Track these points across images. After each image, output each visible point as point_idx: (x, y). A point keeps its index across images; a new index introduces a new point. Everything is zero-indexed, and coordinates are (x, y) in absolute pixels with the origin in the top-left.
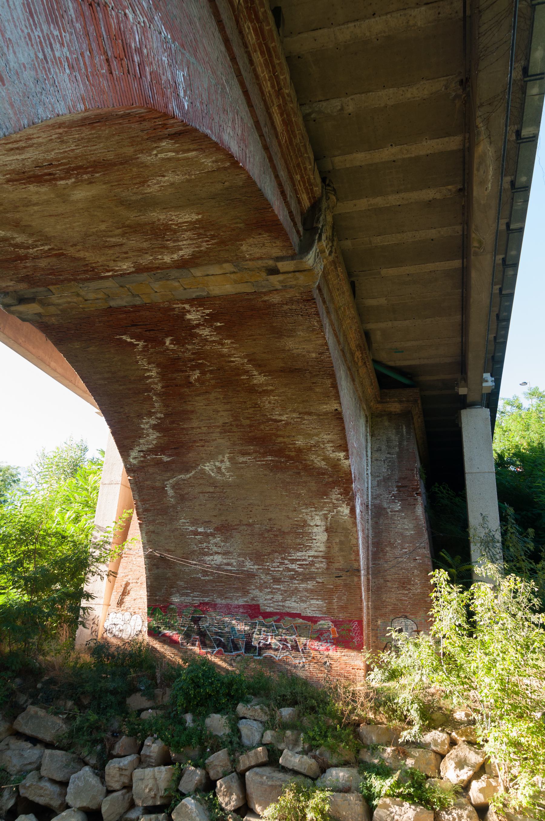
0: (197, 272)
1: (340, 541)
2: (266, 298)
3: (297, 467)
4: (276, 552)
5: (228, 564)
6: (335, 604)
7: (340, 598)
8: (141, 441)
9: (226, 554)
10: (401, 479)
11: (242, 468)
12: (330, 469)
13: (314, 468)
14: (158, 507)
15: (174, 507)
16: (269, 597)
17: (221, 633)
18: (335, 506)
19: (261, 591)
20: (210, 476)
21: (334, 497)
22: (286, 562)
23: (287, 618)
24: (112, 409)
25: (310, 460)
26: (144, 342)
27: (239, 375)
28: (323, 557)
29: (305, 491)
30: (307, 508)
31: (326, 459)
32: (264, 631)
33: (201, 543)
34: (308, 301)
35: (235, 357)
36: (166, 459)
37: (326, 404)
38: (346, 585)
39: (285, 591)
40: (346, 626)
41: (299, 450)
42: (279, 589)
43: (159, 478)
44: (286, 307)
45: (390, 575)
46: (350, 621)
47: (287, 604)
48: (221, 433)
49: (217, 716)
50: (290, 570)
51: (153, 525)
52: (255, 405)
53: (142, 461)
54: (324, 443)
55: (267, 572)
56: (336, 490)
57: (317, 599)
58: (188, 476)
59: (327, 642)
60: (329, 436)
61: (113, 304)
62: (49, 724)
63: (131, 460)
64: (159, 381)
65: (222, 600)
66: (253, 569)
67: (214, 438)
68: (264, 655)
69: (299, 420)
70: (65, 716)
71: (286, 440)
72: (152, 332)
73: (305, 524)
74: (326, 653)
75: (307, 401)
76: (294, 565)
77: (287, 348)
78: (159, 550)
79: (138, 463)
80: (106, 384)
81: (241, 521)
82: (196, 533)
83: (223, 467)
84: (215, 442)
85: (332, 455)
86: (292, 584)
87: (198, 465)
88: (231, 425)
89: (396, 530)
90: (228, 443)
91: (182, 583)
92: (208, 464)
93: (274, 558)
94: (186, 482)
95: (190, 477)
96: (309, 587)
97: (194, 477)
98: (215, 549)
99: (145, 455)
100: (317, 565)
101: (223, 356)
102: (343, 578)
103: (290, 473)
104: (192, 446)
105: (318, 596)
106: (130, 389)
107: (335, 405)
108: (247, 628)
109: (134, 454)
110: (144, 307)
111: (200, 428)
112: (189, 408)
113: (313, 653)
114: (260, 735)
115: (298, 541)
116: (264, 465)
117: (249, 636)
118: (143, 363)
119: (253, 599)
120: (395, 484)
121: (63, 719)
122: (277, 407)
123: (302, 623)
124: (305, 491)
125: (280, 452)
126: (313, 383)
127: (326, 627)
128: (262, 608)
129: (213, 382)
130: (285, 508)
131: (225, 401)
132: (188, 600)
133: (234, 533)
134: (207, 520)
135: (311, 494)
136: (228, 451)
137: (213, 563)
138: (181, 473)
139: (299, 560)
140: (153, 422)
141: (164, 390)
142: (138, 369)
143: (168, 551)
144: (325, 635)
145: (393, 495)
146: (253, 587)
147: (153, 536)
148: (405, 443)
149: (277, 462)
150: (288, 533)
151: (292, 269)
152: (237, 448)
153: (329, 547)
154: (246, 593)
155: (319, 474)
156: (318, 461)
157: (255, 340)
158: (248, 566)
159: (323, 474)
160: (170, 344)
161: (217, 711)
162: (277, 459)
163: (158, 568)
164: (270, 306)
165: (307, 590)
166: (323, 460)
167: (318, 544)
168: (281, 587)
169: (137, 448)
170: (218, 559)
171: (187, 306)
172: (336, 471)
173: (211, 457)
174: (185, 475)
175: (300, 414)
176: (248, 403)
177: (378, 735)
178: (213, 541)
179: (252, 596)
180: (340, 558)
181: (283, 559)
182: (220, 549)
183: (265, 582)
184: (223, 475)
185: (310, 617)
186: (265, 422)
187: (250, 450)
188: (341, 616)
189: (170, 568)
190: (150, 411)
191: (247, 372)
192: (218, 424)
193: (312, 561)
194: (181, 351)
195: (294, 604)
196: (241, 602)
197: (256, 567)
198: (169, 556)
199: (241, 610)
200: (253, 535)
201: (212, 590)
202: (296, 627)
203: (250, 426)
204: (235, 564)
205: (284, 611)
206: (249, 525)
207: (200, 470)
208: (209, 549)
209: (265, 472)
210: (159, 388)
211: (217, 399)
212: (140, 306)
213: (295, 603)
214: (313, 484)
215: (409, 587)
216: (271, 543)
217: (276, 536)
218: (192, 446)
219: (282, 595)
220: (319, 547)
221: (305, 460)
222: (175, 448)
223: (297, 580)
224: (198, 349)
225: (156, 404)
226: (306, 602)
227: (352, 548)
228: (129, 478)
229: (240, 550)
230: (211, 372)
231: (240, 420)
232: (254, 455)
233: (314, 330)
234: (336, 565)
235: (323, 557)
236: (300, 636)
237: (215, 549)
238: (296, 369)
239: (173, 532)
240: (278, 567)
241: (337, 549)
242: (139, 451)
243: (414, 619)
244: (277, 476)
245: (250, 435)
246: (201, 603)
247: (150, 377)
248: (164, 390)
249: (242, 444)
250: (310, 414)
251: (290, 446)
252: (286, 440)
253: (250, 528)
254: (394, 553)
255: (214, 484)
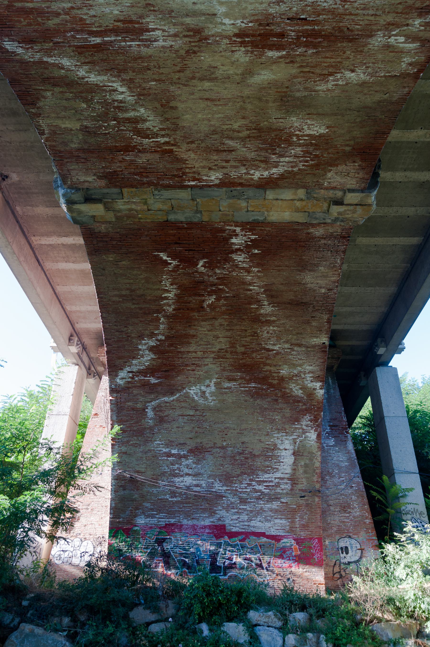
0: (270, 195)
1: (305, 464)
2: (312, 230)
3: (276, 395)
4: (245, 474)
5: (197, 486)
6: (298, 523)
7: (302, 518)
8: (134, 362)
9: (196, 475)
10: (332, 420)
11: (226, 393)
12: (305, 397)
13: (292, 396)
14: (135, 428)
15: (151, 428)
16: (235, 517)
17: (186, 554)
18: (304, 432)
19: (227, 511)
20: (193, 400)
21: (304, 423)
22: (254, 483)
23: (252, 538)
24: (115, 327)
25: (289, 389)
26: (178, 262)
27: (250, 304)
28: (289, 479)
29: (279, 417)
30: (278, 433)
31: (304, 388)
32: (229, 551)
33: (172, 465)
34: (344, 237)
35: (254, 286)
36: (153, 381)
37: (317, 337)
38: (307, 505)
39: (251, 511)
40: (307, 544)
41: (282, 379)
42: (245, 510)
43: (142, 399)
44: (323, 241)
45: (332, 500)
46: (311, 539)
47: (253, 523)
48: (214, 358)
49: (232, 625)
50: (256, 491)
51: (126, 446)
52: (255, 334)
53: (129, 382)
54: (305, 373)
55: (235, 493)
56: (308, 417)
57: (281, 519)
58: (172, 399)
59: (290, 560)
60: (311, 368)
61: (172, 217)
62: (50, 642)
63: (118, 381)
64: (174, 303)
65: (188, 520)
66: (221, 490)
67: (206, 363)
68: (229, 574)
69: (289, 350)
70: (65, 633)
71: (272, 368)
72: (191, 253)
73: (275, 447)
74: (289, 570)
75: (301, 334)
76: (260, 487)
77: (304, 282)
78: (129, 471)
79: (124, 384)
80: (119, 301)
81: (215, 444)
82: (169, 455)
83: (208, 391)
84: (206, 367)
85: (310, 385)
86: (258, 504)
87: (184, 388)
88: (226, 352)
89: (333, 462)
90: (218, 369)
91: (148, 505)
92: (194, 388)
93: (243, 479)
94: (168, 404)
95: (174, 400)
96: (274, 507)
97: (177, 400)
98: (186, 470)
99: (133, 375)
100: (283, 487)
101: (244, 283)
102: (306, 498)
103: (269, 399)
104: (183, 369)
105: (282, 515)
106: (141, 309)
107: (324, 339)
108: (213, 548)
109: (122, 374)
110: (200, 225)
111: (196, 352)
112: (192, 332)
113: (277, 570)
114: (282, 640)
115: (267, 463)
116: (247, 391)
117: (214, 556)
118: (166, 283)
119: (219, 520)
120: (327, 424)
121: (64, 636)
122: (273, 337)
123: (266, 542)
124: (279, 417)
125: (264, 380)
126: (312, 317)
127: (288, 545)
128: (228, 528)
129: (224, 308)
130: (259, 432)
131: (228, 328)
132: (154, 521)
133: (207, 455)
134: (182, 442)
135: (284, 420)
136: (217, 376)
137: (182, 484)
138: (165, 395)
139: (266, 481)
140: (152, 343)
141: (174, 312)
142: (159, 289)
143: (138, 472)
144: (288, 552)
145: (327, 432)
146: (220, 508)
147: (124, 456)
148: (332, 391)
149: (259, 388)
150: (258, 456)
151: (356, 202)
152: (226, 374)
153: (294, 470)
154: (212, 513)
155: (295, 401)
156: (296, 390)
157: (279, 271)
158: (217, 488)
159: (299, 402)
160: (202, 266)
161: (230, 620)
162: (259, 386)
163: (124, 490)
164: (310, 238)
165: (271, 510)
166: (301, 389)
167: (285, 467)
168: (247, 507)
169: (128, 369)
170: (188, 480)
171: (238, 229)
172: (310, 400)
173: (199, 380)
174: (169, 397)
175: (291, 345)
176: (248, 331)
177: (393, 631)
178: (185, 462)
179: (219, 516)
180: (304, 480)
181: (251, 480)
182: (191, 470)
183: (232, 503)
184: (206, 399)
185: (273, 536)
186: (258, 351)
187: (237, 376)
188: (303, 534)
189: (138, 490)
190: (153, 333)
191: (258, 302)
192: (214, 350)
193: (278, 483)
194: (208, 275)
195: (259, 524)
196: (207, 522)
197: (225, 488)
198: (140, 478)
199: (207, 531)
200: (225, 457)
201: (179, 511)
202: (260, 546)
203: (244, 353)
204: (204, 485)
205: (249, 531)
206: (223, 448)
207: (185, 393)
208: (180, 470)
209: (247, 398)
210: (171, 310)
211: (221, 325)
212: (195, 224)
213: (260, 523)
214: (288, 411)
215: (349, 510)
216: (242, 465)
217: (246, 458)
218: (183, 369)
219: (247, 515)
220: (285, 469)
221: (285, 388)
222: (166, 371)
223: (263, 501)
224: (226, 274)
225: (161, 326)
226: (270, 521)
227: (315, 470)
228: (111, 398)
229: (211, 471)
230: (226, 298)
231: (236, 347)
232: (240, 381)
233: (334, 266)
234: (300, 486)
235: (289, 479)
236: (264, 554)
237: (186, 470)
238: (302, 303)
239: (146, 453)
240: (246, 488)
241: (301, 471)
242: (129, 372)
243: (357, 539)
244: (256, 402)
245: (241, 362)
246: (166, 524)
247: (166, 298)
248: (174, 312)
249: (231, 370)
250: (300, 345)
251: (274, 374)
252: (272, 368)
253: (223, 451)
254: (333, 482)
255: (195, 408)
